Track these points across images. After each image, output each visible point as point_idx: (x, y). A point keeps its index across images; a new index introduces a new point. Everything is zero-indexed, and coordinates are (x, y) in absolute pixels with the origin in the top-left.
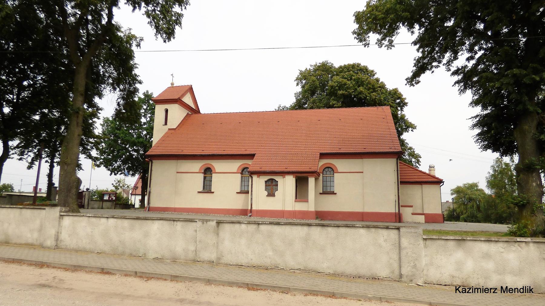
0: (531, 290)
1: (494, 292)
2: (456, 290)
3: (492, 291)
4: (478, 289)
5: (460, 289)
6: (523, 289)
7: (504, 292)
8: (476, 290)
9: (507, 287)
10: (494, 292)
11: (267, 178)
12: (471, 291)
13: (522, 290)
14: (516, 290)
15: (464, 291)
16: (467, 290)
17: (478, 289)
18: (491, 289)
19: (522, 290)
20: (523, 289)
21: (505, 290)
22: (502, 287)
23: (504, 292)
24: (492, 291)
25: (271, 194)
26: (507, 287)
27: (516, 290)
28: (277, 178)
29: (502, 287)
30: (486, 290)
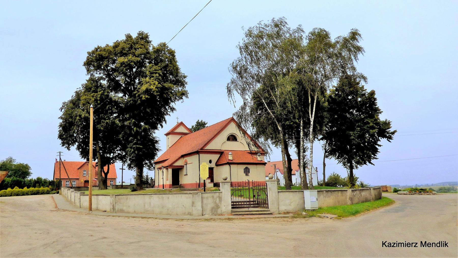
0: (446, 245)
1: (415, 246)
2: (383, 244)
4: (401, 244)
5: (386, 244)
7: (423, 246)
8: (399, 244)
9: (426, 242)
10: (415, 246)
11: (245, 166)
12: (395, 245)
13: (438, 245)
14: (434, 244)
15: (390, 245)
16: (392, 245)
17: (401, 244)
19: (438, 245)
21: (424, 244)
22: (421, 242)
23: (423, 246)
25: (247, 175)
26: (426, 242)
27: (434, 244)
28: (249, 166)
29: (421, 242)
30: (408, 245)
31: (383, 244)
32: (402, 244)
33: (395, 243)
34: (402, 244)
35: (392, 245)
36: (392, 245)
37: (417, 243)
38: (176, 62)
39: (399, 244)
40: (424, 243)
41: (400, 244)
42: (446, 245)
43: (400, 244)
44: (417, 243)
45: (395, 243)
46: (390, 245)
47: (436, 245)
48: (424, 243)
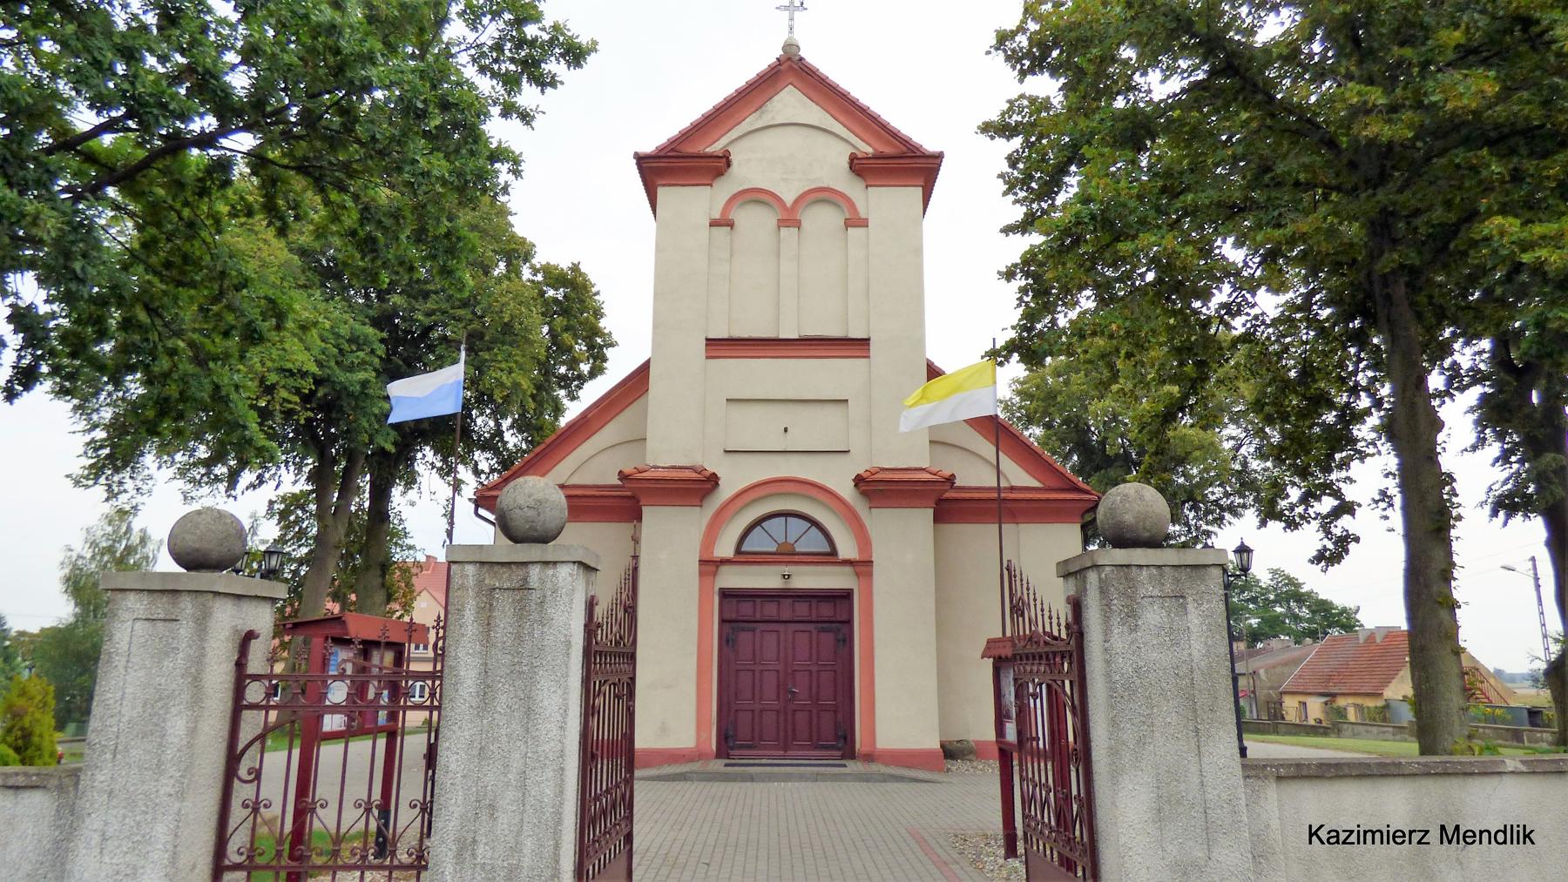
0: (1526, 836)
2: (1311, 835)
3: (1416, 837)
4: (1373, 833)
5: (1323, 834)
6: (1505, 832)
9: (1457, 828)
10: (1419, 842)
12: (1353, 838)
13: (1501, 837)
14: (1485, 835)
15: (1335, 838)
16: (1343, 836)
19: (1501, 837)
20: (1505, 832)
22: (1443, 828)
24: (1416, 837)
26: (1457, 828)
27: (1485, 835)
29: (1443, 828)
30: (1396, 837)
31: (1313, 834)
32: (1378, 835)
33: (1352, 832)
34: (1378, 835)
38: (598, 314)
40: (1450, 831)
41: (1369, 835)
42: (1526, 836)
43: (1369, 835)
45: (1352, 832)
46: (1335, 838)
47: (1493, 837)
48: (1450, 831)
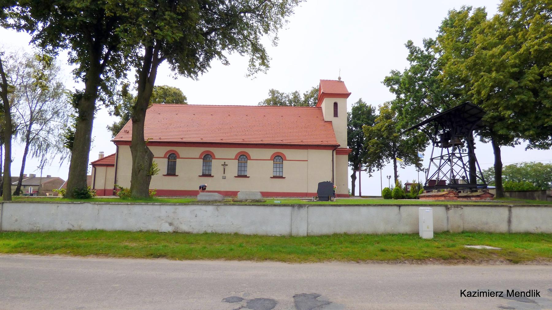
0: (537, 294)
2: (461, 294)
4: (483, 293)
5: (466, 293)
8: (480, 294)
9: (513, 291)
12: (476, 295)
13: (528, 294)
14: (523, 294)
15: (470, 294)
18: (497, 292)
19: (528, 294)
22: (508, 291)
26: (513, 291)
27: (523, 294)
29: (508, 291)
31: (462, 293)
32: (485, 293)
34: (485, 293)
35: (472, 295)
36: (472, 295)
37: (502, 292)
39: (480, 294)
41: (482, 294)
42: (537, 294)
43: (482, 294)
44: (502, 292)
